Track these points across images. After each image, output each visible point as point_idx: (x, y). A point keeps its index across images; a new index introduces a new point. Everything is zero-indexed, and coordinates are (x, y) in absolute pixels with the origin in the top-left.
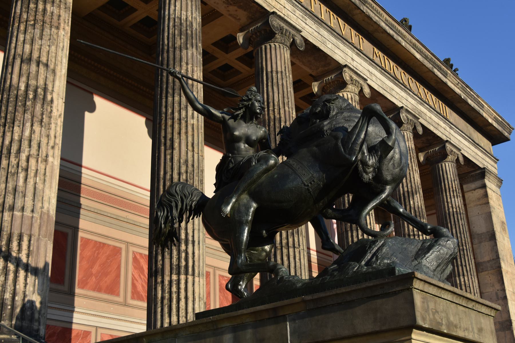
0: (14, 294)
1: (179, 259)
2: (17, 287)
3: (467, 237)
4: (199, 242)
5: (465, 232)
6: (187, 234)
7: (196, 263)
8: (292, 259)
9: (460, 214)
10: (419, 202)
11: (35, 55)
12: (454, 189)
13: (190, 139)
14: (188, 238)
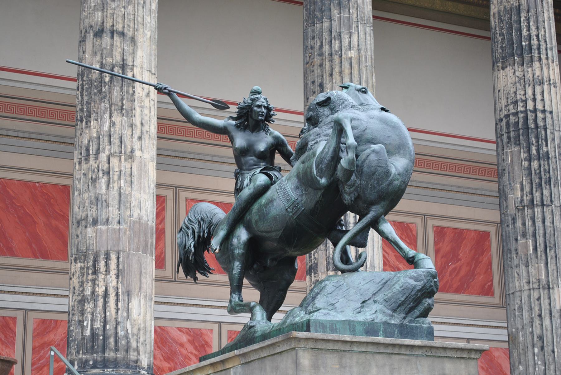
0: (105, 323)
2: (108, 314)
8: (539, 224)
11: (108, 25)
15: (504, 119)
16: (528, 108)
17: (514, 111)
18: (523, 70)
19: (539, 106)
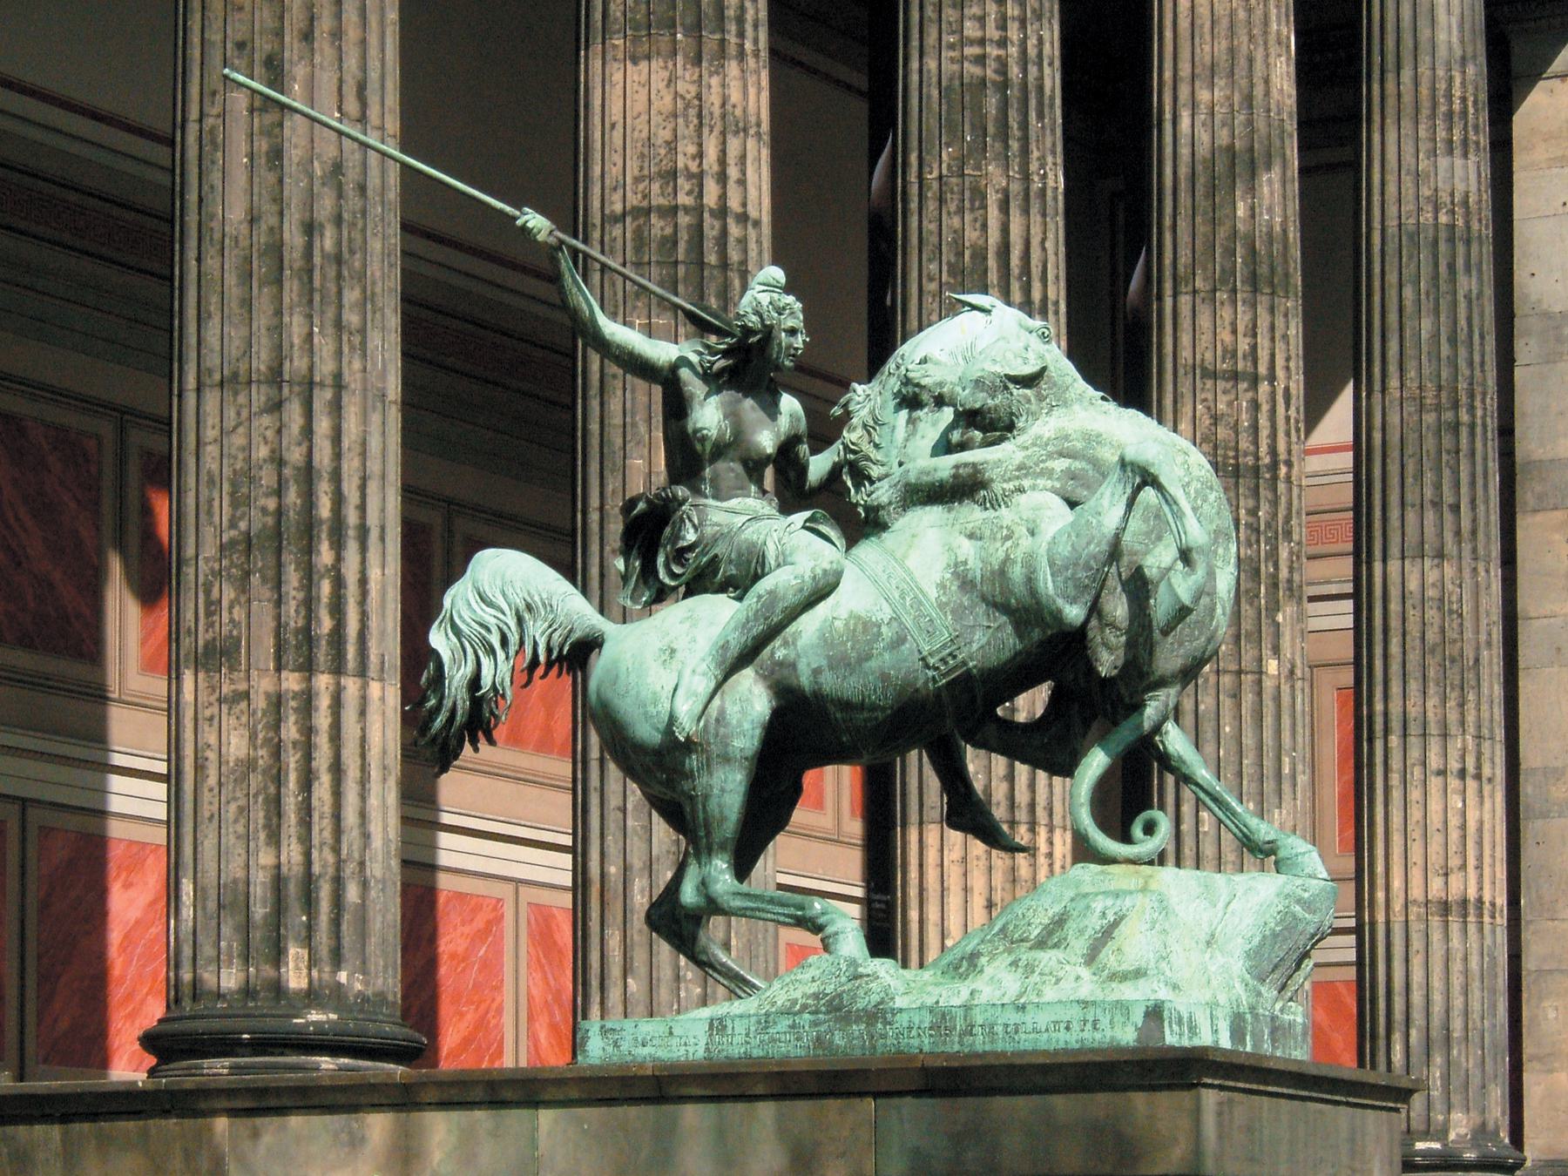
1: (309, 604)
3: (1482, 364)
4: (383, 528)
5: (1476, 337)
6: (338, 500)
7: (373, 623)
9: (1468, 242)
10: (1278, 210)
12: (1457, 106)
13: (351, 63)
14: (345, 516)
15: (628, 219)
16: (705, 201)
17: (662, 201)
18: (696, 77)
19: (734, 203)
